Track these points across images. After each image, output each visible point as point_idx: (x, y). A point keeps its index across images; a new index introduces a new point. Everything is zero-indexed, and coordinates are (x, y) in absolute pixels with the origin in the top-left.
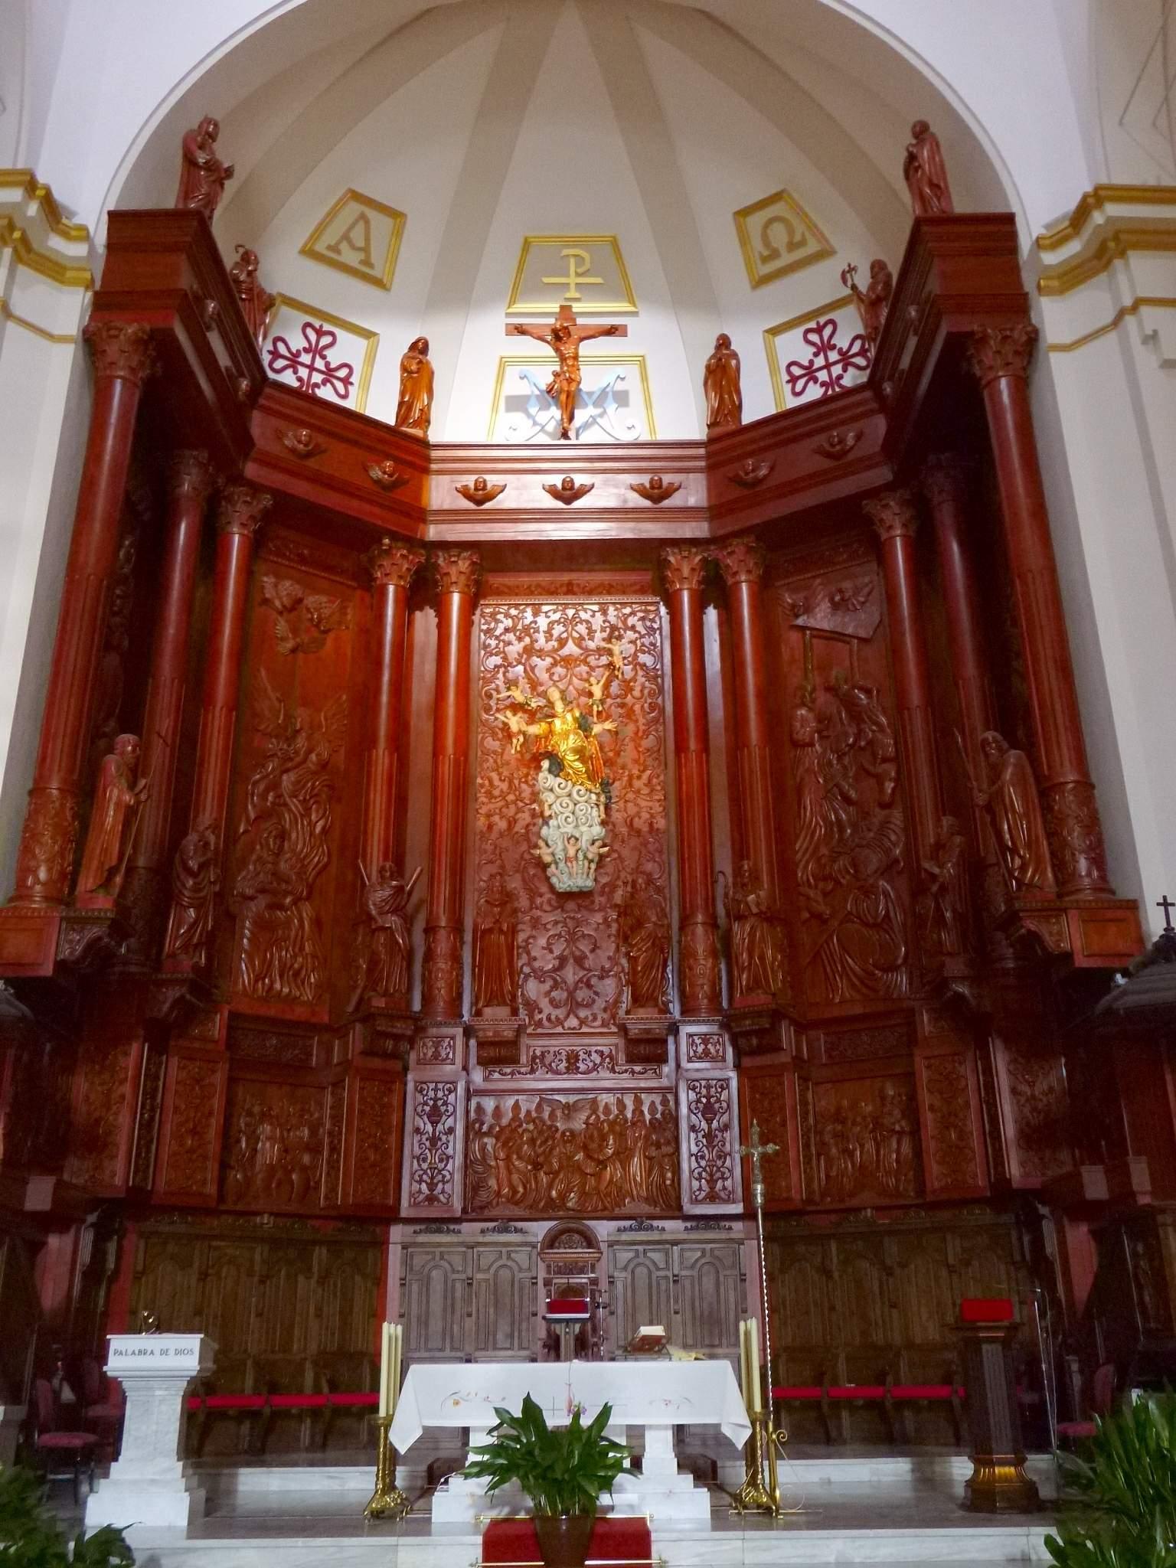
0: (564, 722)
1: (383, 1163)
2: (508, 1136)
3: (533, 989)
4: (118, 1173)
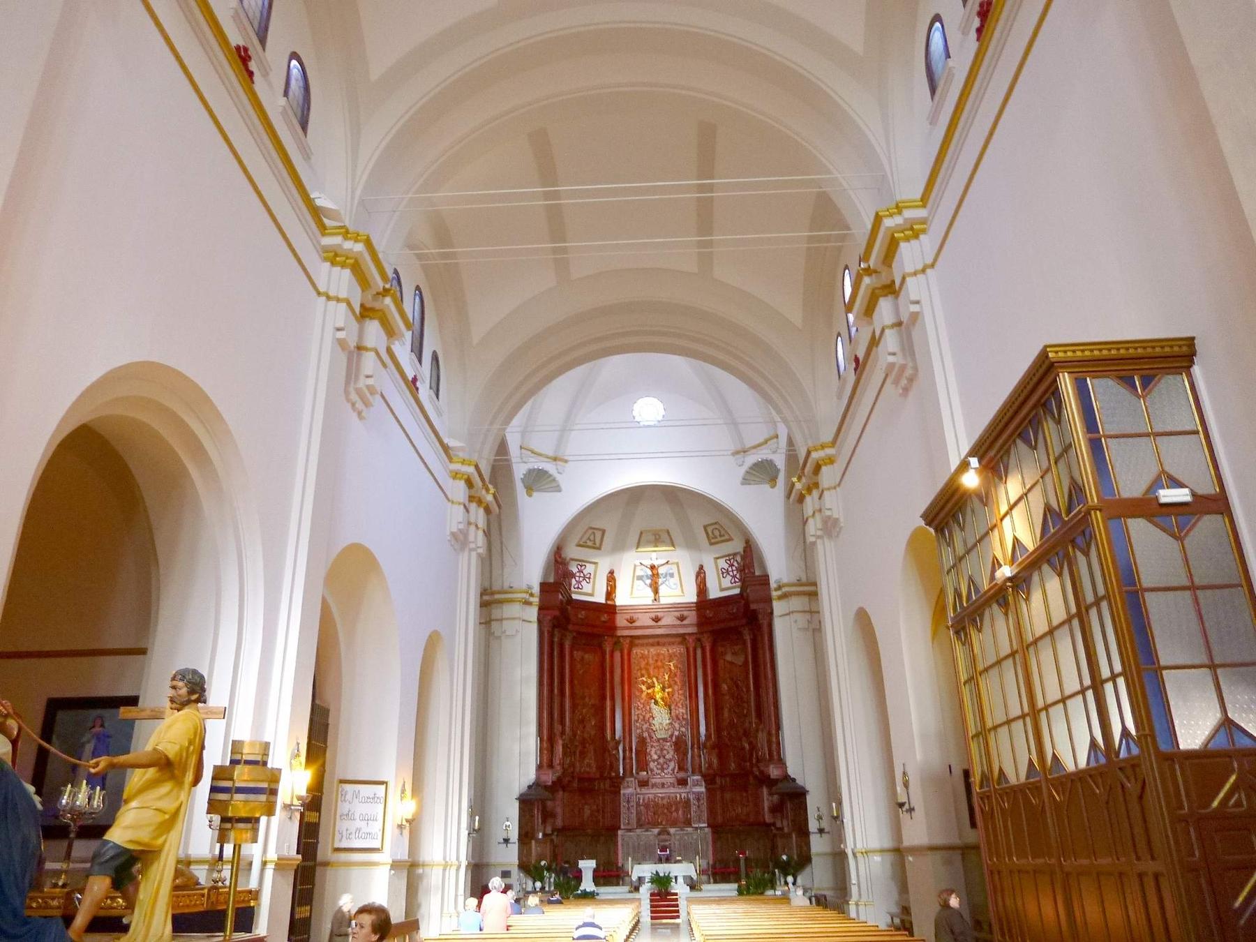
0: (658, 688)
1: (616, 814)
2: (647, 806)
3: (652, 765)
4: (559, 823)
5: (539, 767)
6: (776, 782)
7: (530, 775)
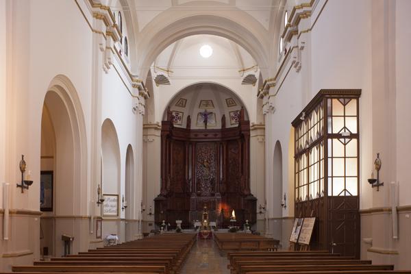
4: (168, 208)
5: (162, 189)
6: (247, 195)
7: (159, 193)
